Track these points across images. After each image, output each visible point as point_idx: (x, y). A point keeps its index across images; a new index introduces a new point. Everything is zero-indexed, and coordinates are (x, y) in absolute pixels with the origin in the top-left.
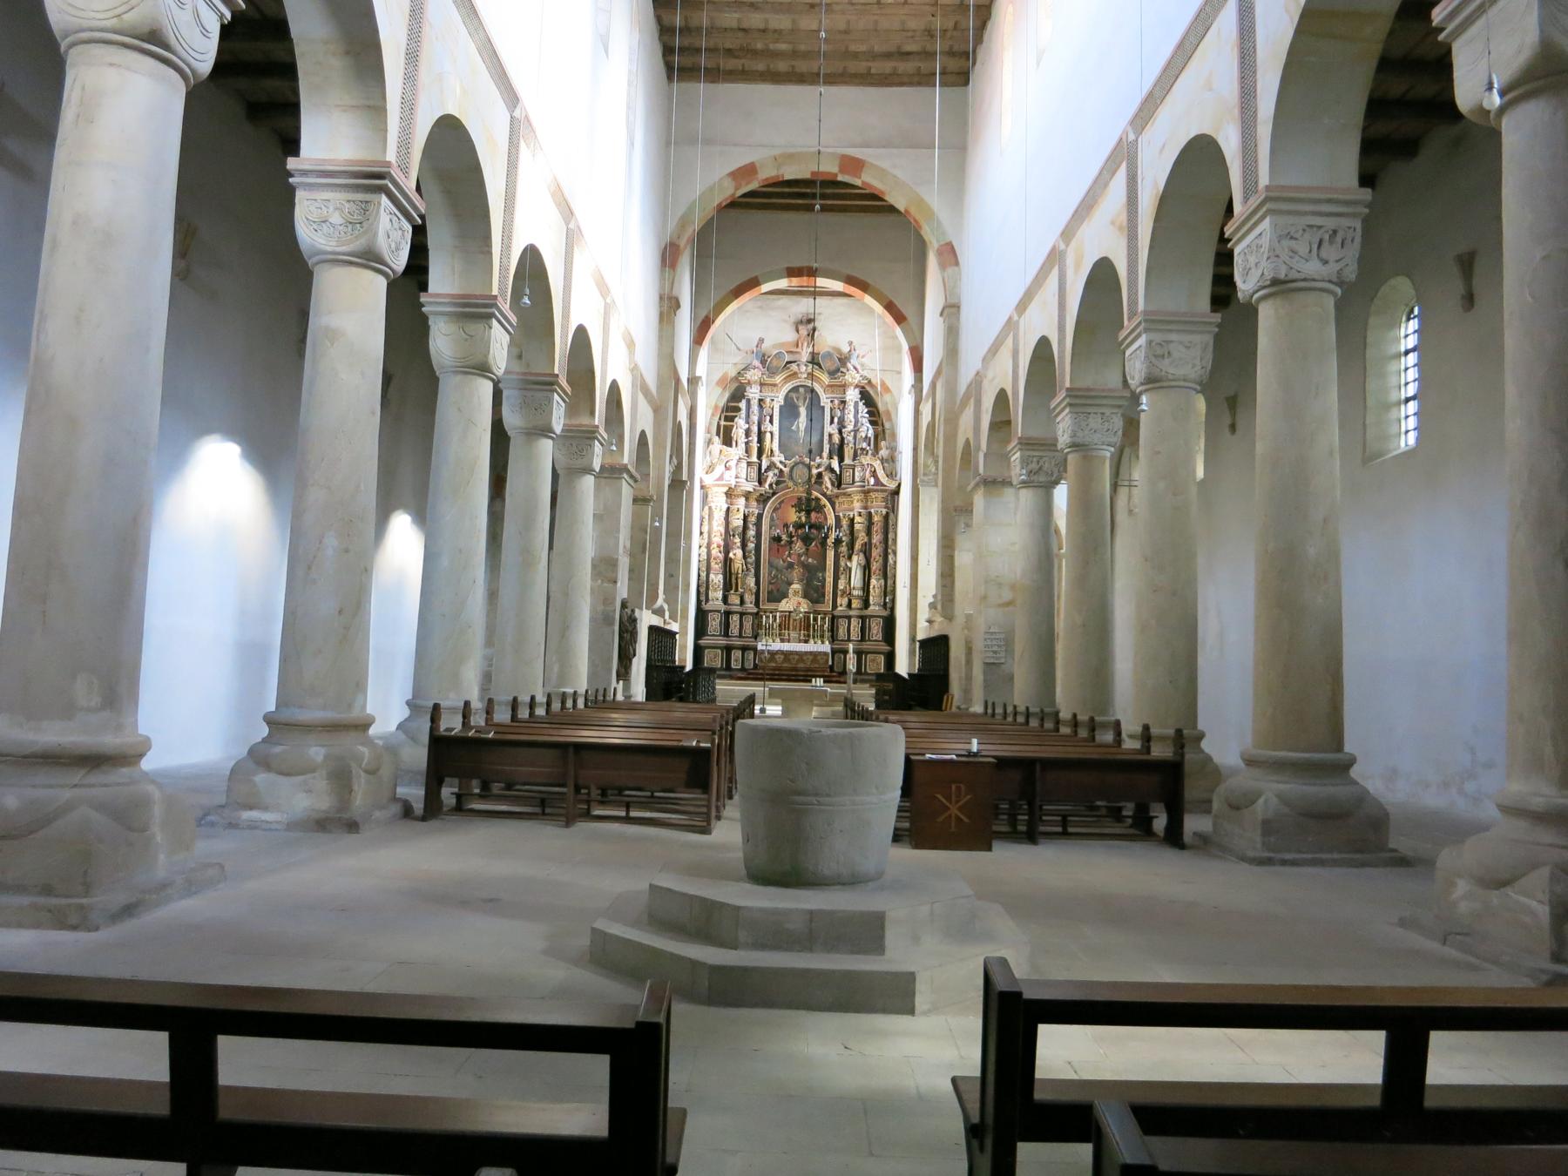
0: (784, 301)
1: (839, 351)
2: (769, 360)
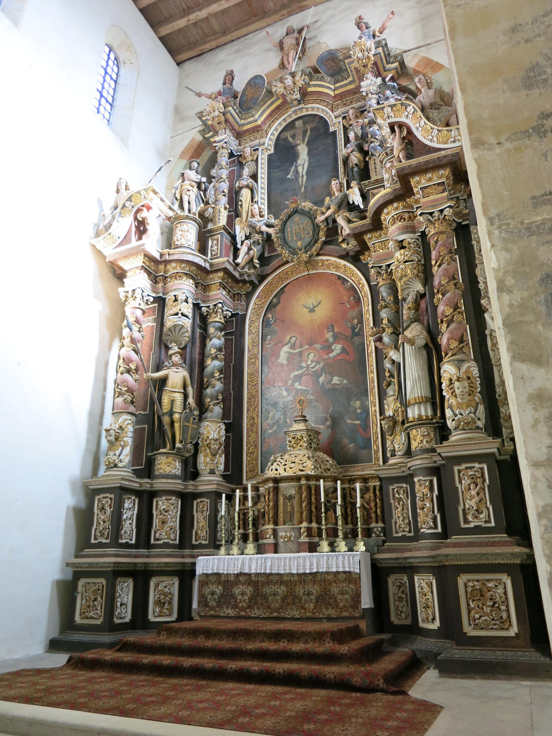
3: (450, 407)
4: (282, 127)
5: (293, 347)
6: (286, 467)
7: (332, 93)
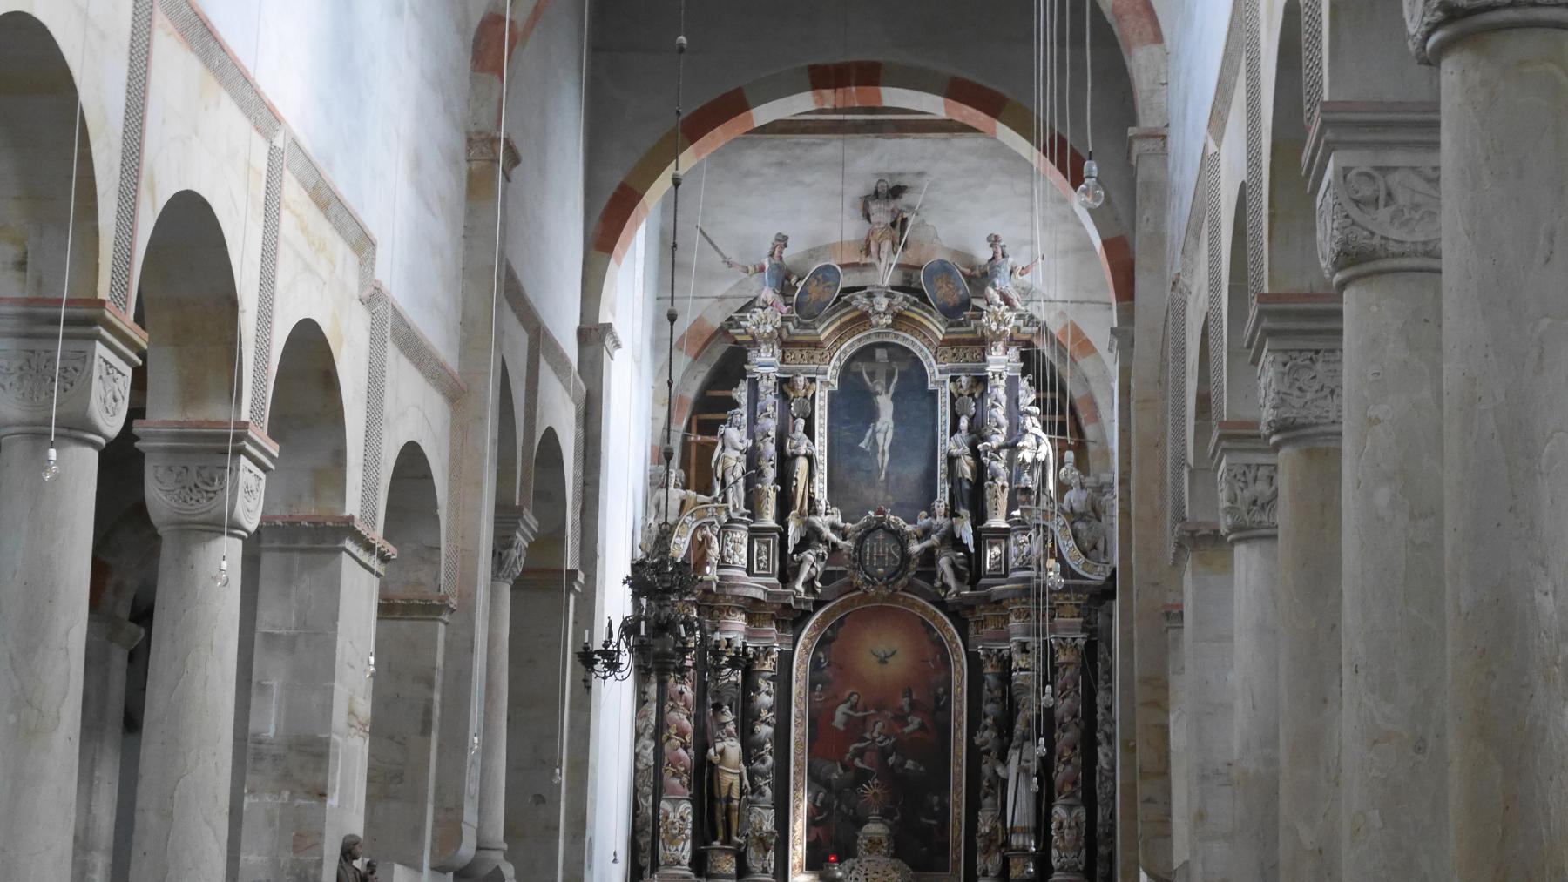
0: (832, 147)
1: (967, 258)
2: (800, 285)
3: (1058, 848)
4: (855, 349)
5: (854, 707)
6: (868, 876)
7: (941, 337)
